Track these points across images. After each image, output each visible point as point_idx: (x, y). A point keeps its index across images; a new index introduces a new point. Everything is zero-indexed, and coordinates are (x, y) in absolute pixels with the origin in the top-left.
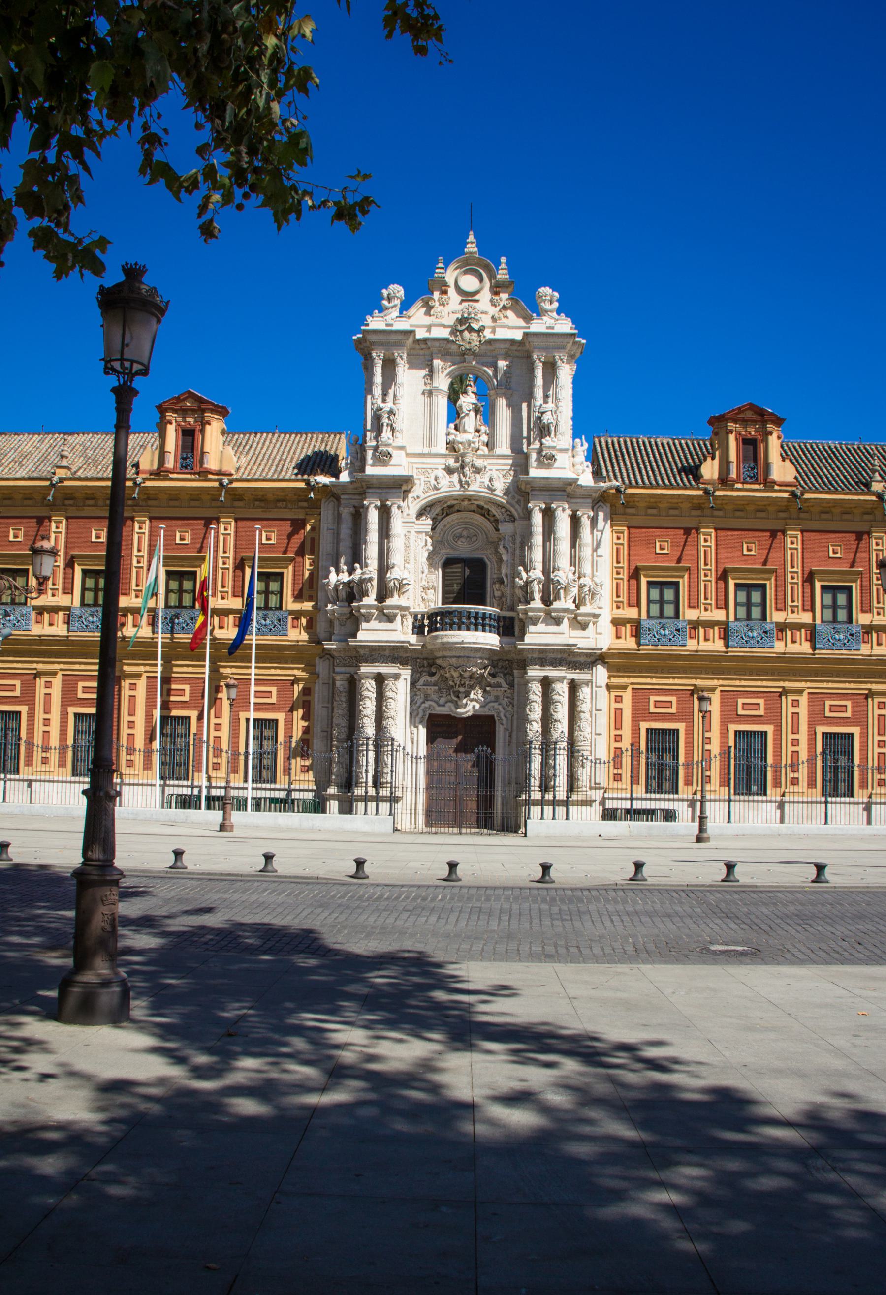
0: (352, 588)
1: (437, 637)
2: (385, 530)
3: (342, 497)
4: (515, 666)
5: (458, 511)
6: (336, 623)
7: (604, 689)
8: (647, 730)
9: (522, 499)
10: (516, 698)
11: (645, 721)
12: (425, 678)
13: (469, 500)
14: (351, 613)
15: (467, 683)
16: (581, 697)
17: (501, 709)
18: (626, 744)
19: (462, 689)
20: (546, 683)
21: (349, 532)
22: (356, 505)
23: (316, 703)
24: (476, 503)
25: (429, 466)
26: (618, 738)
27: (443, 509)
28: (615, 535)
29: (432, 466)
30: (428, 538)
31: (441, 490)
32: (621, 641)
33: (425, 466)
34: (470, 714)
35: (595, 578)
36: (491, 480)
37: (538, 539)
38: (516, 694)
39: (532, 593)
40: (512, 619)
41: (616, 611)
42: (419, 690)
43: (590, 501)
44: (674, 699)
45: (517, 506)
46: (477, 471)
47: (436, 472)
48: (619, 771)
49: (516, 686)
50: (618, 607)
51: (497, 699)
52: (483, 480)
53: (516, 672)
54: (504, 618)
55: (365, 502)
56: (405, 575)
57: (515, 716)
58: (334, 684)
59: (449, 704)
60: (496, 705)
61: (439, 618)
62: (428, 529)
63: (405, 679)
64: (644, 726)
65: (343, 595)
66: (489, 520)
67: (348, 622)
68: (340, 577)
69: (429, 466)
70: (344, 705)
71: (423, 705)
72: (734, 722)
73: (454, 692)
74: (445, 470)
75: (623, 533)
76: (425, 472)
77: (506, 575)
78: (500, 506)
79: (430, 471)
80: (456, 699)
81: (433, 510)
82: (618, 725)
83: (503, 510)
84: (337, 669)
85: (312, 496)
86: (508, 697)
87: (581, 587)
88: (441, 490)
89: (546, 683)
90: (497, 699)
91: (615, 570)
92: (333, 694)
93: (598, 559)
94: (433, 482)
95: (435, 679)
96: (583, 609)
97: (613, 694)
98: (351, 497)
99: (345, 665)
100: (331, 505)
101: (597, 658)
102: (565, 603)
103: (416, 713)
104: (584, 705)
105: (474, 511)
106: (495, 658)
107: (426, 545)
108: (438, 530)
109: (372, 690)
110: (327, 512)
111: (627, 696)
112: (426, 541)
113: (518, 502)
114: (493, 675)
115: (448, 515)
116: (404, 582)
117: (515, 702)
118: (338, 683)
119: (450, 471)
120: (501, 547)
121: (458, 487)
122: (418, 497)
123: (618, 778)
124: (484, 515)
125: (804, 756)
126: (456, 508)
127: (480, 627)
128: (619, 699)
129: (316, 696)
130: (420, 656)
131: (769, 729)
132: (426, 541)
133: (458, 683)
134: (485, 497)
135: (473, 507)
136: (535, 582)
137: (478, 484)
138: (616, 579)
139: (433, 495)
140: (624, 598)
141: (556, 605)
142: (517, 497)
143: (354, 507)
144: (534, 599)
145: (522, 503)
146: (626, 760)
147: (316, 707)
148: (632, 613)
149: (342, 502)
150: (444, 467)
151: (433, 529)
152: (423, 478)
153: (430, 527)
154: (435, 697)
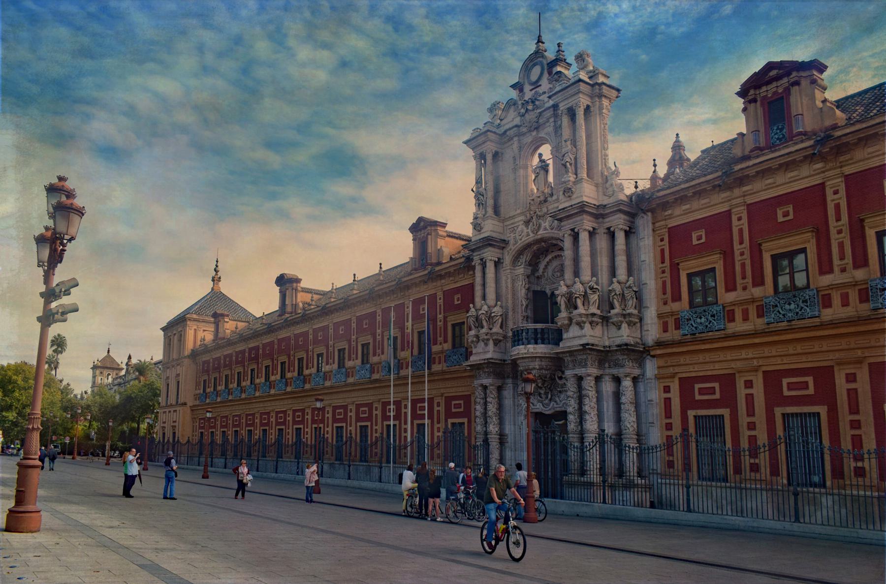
8: (695, 417)
11: (693, 409)
18: (676, 431)
26: (669, 427)
32: (668, 334)
44: (716, 385)
48: (671, 458)
64: (691, 413)
72: (779, 405)
82: (668, 415)
111: (675, 386)
121: (532, 235)
123: (670, 464)
125: (763, 439)
127: (539, 341)
131: (822, 410)
139: (520, 244)
140: (669, 295)
146: (678, 449)
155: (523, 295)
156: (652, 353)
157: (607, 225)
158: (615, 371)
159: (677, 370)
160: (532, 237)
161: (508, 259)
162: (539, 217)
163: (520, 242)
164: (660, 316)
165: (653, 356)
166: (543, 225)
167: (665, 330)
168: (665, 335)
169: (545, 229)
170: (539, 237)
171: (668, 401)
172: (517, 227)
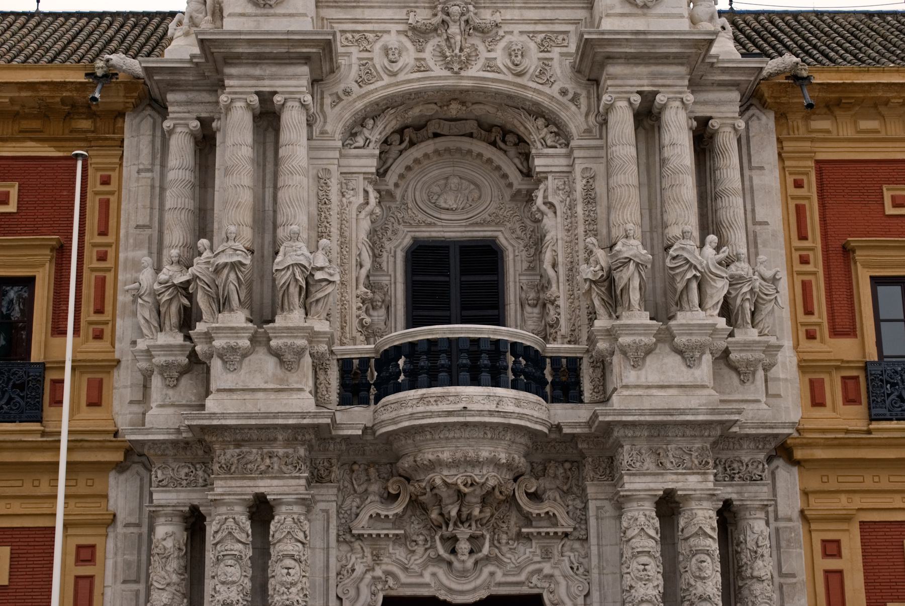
0: (190, 297)
1: (401, 403)
2: (270, 167)
3: (170, 97)
4: (588, 471)
5: (436, 135)
6: (156, 382)
7: (798, 524)
9: (584, 94)
10: (594, 550)
12: (374, 507)
13: (463, 103)
14: (193, 355)
15: (476, 512)
16: (751, 544)
17: (561, 580)
19: (463, 532)
20: (668, 506)
21: (188, 176)
22: (203, 115)
23: (109, 580)
24: (478, 110)
25: (369, 27)
27: (400, 131)
28: (790, 180)
29: (376, 27)
30: (370, 189)
31: (401, 77)
33: (360, 27)
34: (483, 594)
35: (762, 269)
36: (510, 52)
37: (628, 176)
38: (593, 540)
39: (626, 289)
40: (574, 364)
41: (805, 344)
42: (360, 537)
43: (735, 96)
45: (573, 108)
46: (482, 31)
47: (386, 38)
49: (592, 522)
50: (810, 336)
51: (547, 555)
52: (492, 55)
53: (591, 490)
54: (556, 360)
55: (223, 98)
56: (320, 260)
57: (595, 595)
58: (151, 530)
59: (431, 569)
60: (547, 568)
61: (401, 362)
62: (371, 165)
63: (326, 511)
65: (173, 317)
66: (505, 152)
67: (185, 381)
68: (162, 277)
69: (369, 27)
70: (175, 578)
71: (368, 576)
73: (443, 539)
74: (404, 33)
75: (807, 174)
76: (360, 38)
77: (554, 266)
78: (537, 112)
79: (371, 36)
80: (446, 555)
81: (380, 124)
83: (541, 122)
84: (159, 497)
85: (97, 95)
86: (572, 550)
87: (735, 281)
88: (401, 77)
89: (668, 506)
90: (547, 555)
91: (796, 255)
92: (150, 555)
93: (758, 228)
94: (379, 60)
95: (397, 508)
96: (740, 336)
97: (817, 538)
98: (191, 95)
99: (176, 483)
100: (147, 125)
101: (783, 450)
102: (699, 318)
103: (352, 593)
104: (759, 563)
105: (471, 135)
106: (538, 457)
107: (367, 203)
108: (392, 178)
109: (242, 537)
110: (137, 137)
112: (366, 192)
113: (574, 100)
114: (535, 497)
115: (412, 144)
116: (319, 275)
117: (594, 561)
118: (161, 531)
119: (419, 34)
120: (539, 201)
121: (438, 70)
122: (347, 93)
124: (494, 144)
126: (432, 128)
128: (832, 548)
129: (110, 563)
130: (358, 458)
132: (366, 192)
133: (454, 513)
134: (497, 93)
135: (471, 126)
136: (632, 266)
137: (481, 62)
138: (799, 273)
139: (382, 88)
140: (821, 316)
141: (682, 318)
142: (571, 87)
143: (198, 119)
144: (630, 308)
145: (583, 101)
147: (108, 592)
148: (845, 349)
149: (170, 109)
150: (401, 27)
151: (382, 173)
152: (354, 50)
153: (374, 162)
154: (400, 553)
155: (363, 236)
156: (799, 454)
157: (703, 111)
158: (728, 492)
159: (858, 502)
160: (438, 76)
161: (336, 121)
162: (471, 28)
163: (387, 80)
164: (804, 367)
165: (797, 463)
166: (484, 54)
167: (817, 400)
168: (818, 412)
169: (490, 66)
170: (466, 84)
171: (834, 579)
172: (378, 34)
